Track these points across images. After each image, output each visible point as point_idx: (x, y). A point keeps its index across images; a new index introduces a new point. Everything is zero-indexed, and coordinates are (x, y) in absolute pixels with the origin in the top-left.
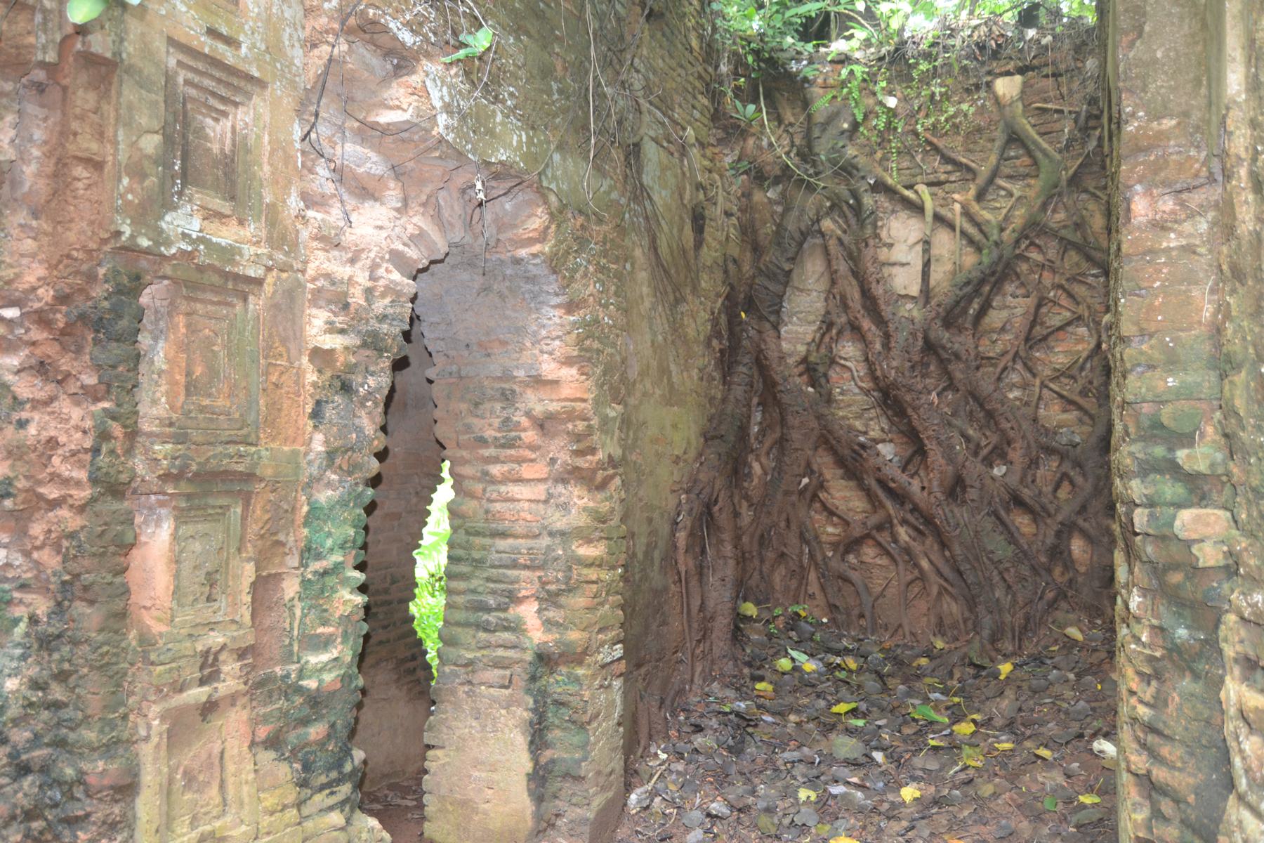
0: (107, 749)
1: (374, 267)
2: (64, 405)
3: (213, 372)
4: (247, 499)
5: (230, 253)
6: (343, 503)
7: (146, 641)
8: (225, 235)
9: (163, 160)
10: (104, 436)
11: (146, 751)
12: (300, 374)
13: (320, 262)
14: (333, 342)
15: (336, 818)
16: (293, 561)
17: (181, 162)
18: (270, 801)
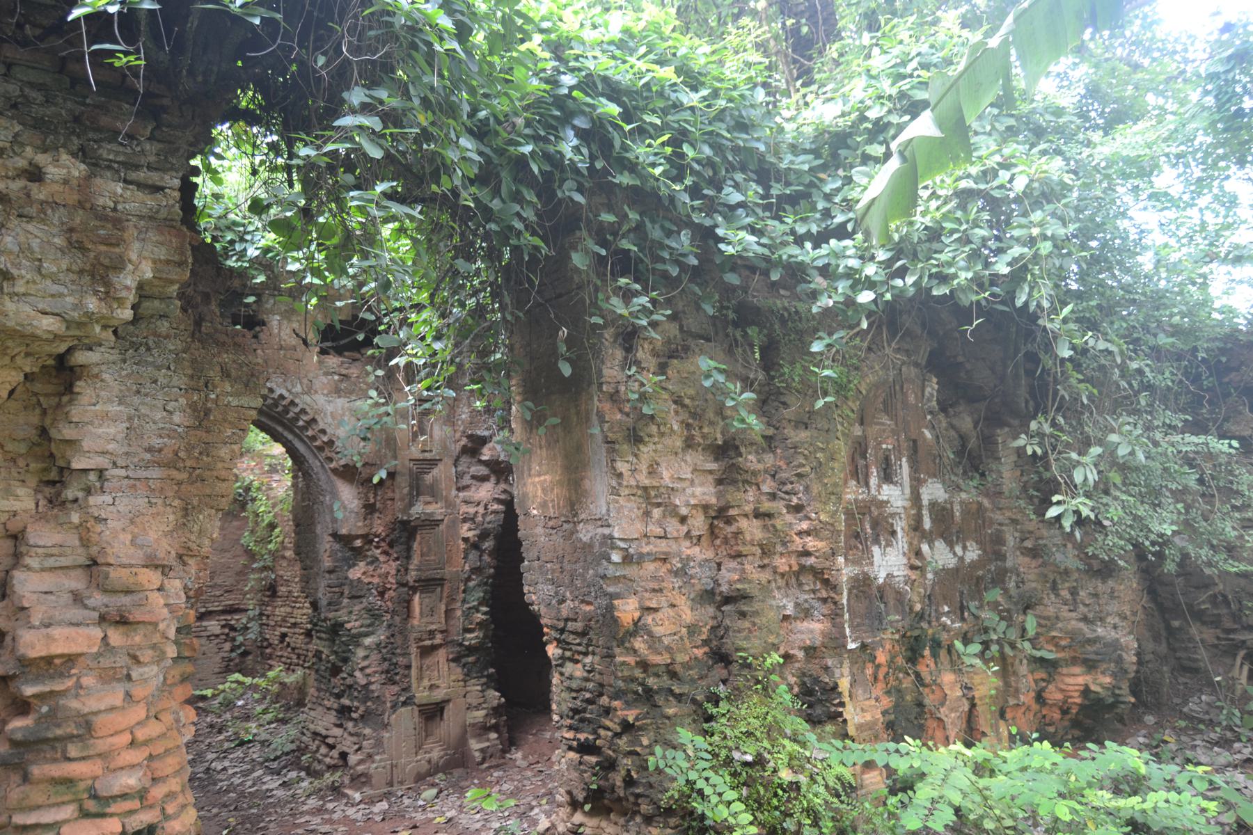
0: (404, 655)
1: (486, 506)
2: (391, 562)
3: (430, 550)
4: (442, 585)
5: (432, 514)
6: (479, 585)
7: (412, 627)
8: (430, 509)
9: (410, 494)
10: (398, 571)
11: (413, 656)
12: (458, 546)
13: (464, 509)
14: (470, 534)
15: (479, 688)
16: (459, 604)
17: (418, 489)
18: (453, 677)
